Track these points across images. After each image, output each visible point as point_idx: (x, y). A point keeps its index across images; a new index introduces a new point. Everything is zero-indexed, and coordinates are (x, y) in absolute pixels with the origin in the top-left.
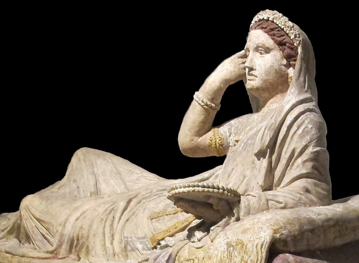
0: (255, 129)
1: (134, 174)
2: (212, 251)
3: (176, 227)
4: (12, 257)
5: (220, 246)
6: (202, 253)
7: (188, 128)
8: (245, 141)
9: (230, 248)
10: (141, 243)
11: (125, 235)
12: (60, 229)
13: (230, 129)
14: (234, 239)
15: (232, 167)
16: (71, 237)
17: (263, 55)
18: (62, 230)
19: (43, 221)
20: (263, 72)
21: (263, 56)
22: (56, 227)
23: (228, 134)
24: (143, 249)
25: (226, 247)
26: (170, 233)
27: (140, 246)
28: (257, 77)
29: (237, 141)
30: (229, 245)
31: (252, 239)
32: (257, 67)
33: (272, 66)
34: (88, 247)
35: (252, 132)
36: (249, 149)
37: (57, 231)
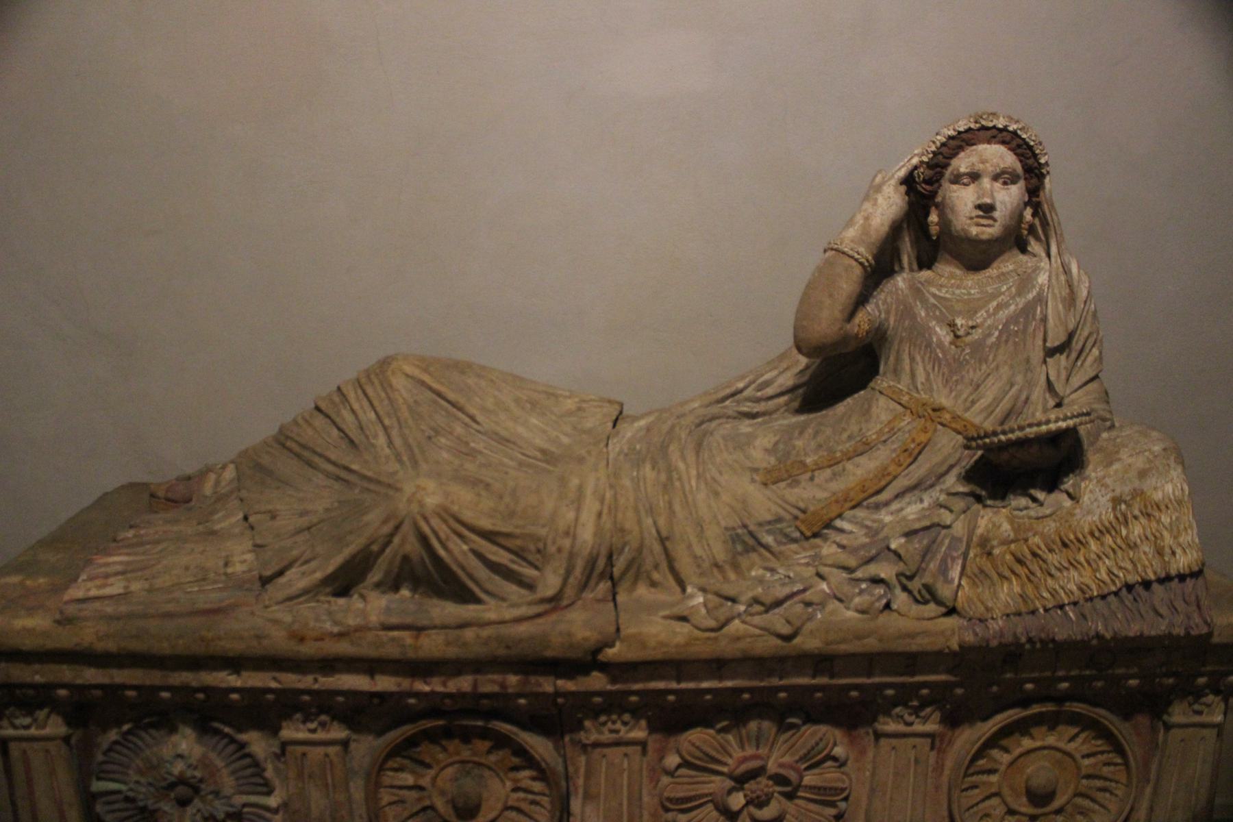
0: (1012, 308)
1: (561, 399)
2: (1078, 517)
3: (865, 489)
4: (417, 637)
5: (1098, 507)
6: (1053, 525)
7: (841, 308)
8: (1000, 327)
9: (1118, 507)
10: (769, 532)
11: (723, 523)
12: (567, 543)
13: (877, 305)
14: (1127, 489)
15: (988, 371)
16: (595, 552)
17: (1009, 187)
18: (572, 547)
19: (508, 535)
20: (1008, 213)
21: (1008, 189)
22: (554, 543)
23: (877, 314)
24: (779, 543)
25: (1110, 505)
26: (853, 503)
27: (769, 539)
28: (995, 220)
29: (973, 327)
30: (1116, 501)
31: (1159, 485)
32: (998, 205)
33: (1018, 205)
34: (639, 568)
35: (1006, 312)
36: (1017, 340)
37: (560, 550)
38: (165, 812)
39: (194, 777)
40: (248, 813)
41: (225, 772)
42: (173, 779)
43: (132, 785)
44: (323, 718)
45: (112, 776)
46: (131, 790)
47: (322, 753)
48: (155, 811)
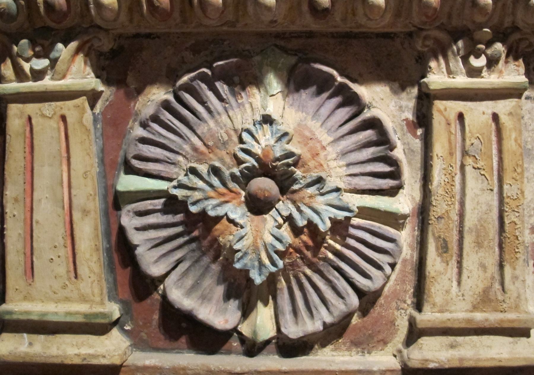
38: (232, 221)
39: (290, 155)
40: (358, 227)
41: (332, 152)
42: (251, 162)
43: (182, 178)
44: (499, 47)
45: (151, 167)
46: (181, 186)
47: (490, 112)
48: (218, 219)
